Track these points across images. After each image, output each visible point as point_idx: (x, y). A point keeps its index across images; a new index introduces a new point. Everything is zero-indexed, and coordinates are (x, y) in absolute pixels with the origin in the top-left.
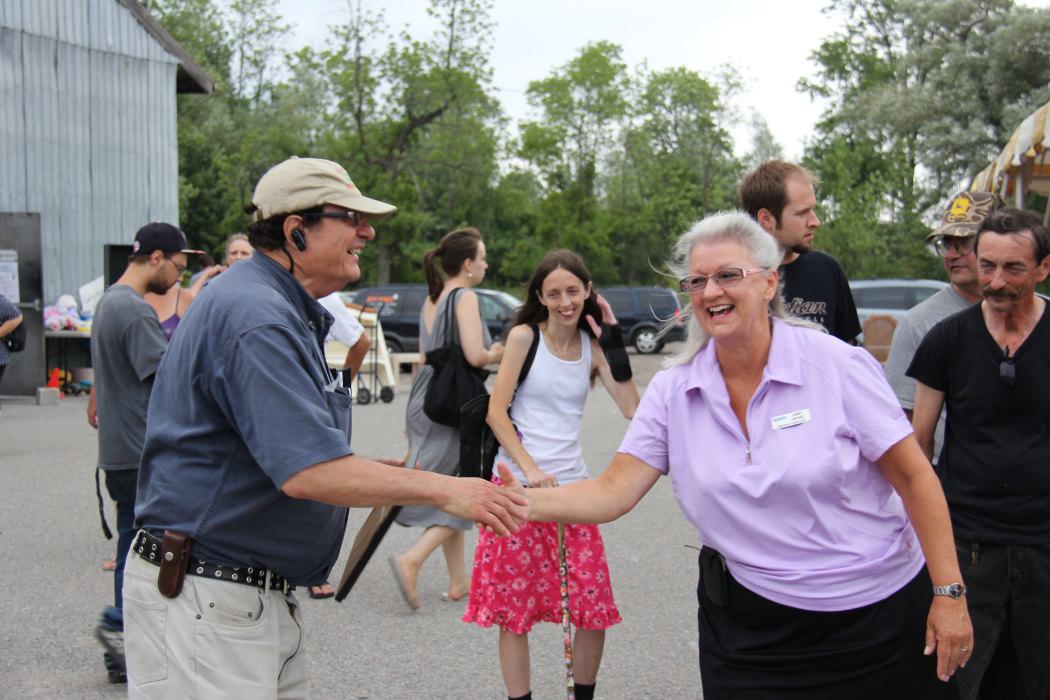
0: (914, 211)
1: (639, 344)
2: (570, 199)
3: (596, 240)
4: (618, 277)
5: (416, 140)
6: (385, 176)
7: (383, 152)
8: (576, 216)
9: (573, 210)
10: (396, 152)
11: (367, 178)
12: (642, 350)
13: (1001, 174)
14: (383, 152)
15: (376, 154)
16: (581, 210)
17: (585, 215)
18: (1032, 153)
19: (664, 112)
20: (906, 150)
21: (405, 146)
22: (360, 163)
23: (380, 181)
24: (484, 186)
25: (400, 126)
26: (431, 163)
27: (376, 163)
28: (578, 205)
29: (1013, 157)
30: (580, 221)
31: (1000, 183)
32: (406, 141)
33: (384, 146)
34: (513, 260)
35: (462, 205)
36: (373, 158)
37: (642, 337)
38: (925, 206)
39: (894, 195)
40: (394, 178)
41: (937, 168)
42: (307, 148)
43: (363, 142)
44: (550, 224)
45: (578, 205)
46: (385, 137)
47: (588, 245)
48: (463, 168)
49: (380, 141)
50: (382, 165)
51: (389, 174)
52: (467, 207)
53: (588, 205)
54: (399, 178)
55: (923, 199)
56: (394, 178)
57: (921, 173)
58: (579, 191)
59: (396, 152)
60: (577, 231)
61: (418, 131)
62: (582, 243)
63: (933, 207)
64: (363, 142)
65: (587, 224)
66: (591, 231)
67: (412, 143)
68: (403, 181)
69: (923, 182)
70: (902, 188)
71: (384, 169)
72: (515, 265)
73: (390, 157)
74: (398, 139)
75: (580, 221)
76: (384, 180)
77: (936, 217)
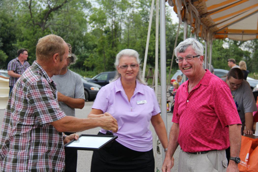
2: (109, 39)
5: (52, 17)
6: (40, 29)
7: (39, 20)
8: (111, 45)
9: (110, 43)
10: (44, 21)
11: (34, 30)
14: (39, 20)
15: (37, 21)
19: (147, 7)
21: (47, 19)
22: (31, 25)
23: (38, 32)
24: (80, 34)
25: (46, 11)
26: (57, 25)
27: (37, 24)
28: (112, 41)
30: (112, 47)
32: (48, 16)
33: (40, 18)
34: (88, 61)
35: (72, 40)
36: (35, 23)
40: (43, 30)
42: (13, 18)
43: (32, 17)
44: (101, 48)
45: (112, 41)
46: (40, 15)
48: (70, 27)
49: (38, 16)
50: (39, 26)
51: (42, 28)
52: (73, 40)
53: (116, 41)
54: (45, 30)
56: (43, 30)
58: (112, 36)
59: (44, 21)
60: (111, 51)
61: (52, 13)
62: (113, 55)
64: (32, 17)
65: (115, 48)
67: (51, 17)
68: (47, 31)
71: (40, 26)
72: (89, 63)
73: (42, 23)
74: (45, 16)
75: (112, 47)
76: (40, 31)
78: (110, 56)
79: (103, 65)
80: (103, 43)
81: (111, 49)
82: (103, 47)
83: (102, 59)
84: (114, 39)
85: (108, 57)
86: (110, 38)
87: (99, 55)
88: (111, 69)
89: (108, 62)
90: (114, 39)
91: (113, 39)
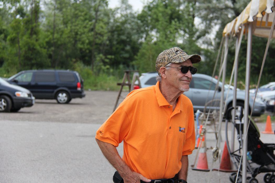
0: (194, 39)
1: (59, 99)
3: (40, 45)
4: (50, 64)
8: (29, 31)
12: (60, 102)
13: (241, 25)
16: (32, 29)
17: (34, 32)
18: (259, 15)
20: (191, 9)
29: (249, 17)
31: (240, 30)
37: (60, 95)
38: (199, 37)
39: (185, 31)
41: (205, 18)
45: (30, 26)
47: (35, 47)
53: (36, 26)
55: (198, 34)
57: (197, 21)
58: (31, 20)
60: (29, 40)
62: (32, 47)
63: (202, 37)
65: (34, 36)
66: (37, 40)
69: (198, 25)
70: (188, 27)
75: (31, 34)
77: (204, 43)
78: (27, 47)
79: (17, 59)
80: (16, 28)
81: (30, 38)
82: (18, 33)
83: (14, 51)
84: (34, 24)
85: (24, 49)
86: (28, 22)
87: (11, 45)
88: (28, 65)
89: (24, 56)
90: (34, 24)
91: (32, 23)
